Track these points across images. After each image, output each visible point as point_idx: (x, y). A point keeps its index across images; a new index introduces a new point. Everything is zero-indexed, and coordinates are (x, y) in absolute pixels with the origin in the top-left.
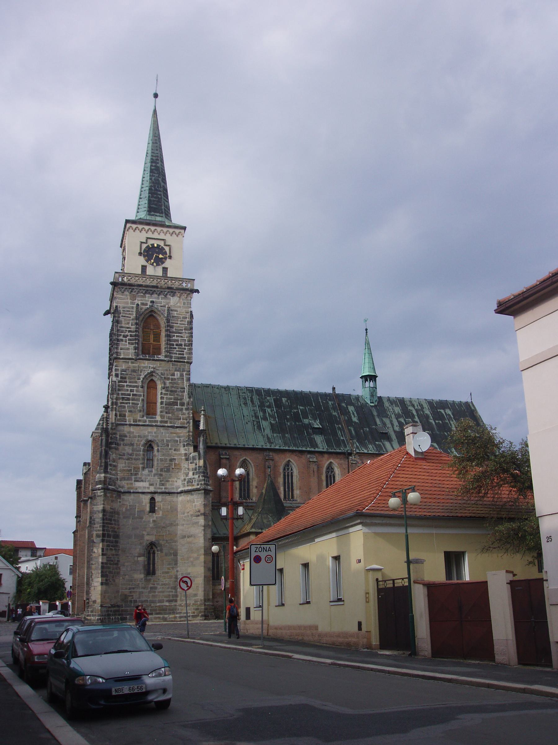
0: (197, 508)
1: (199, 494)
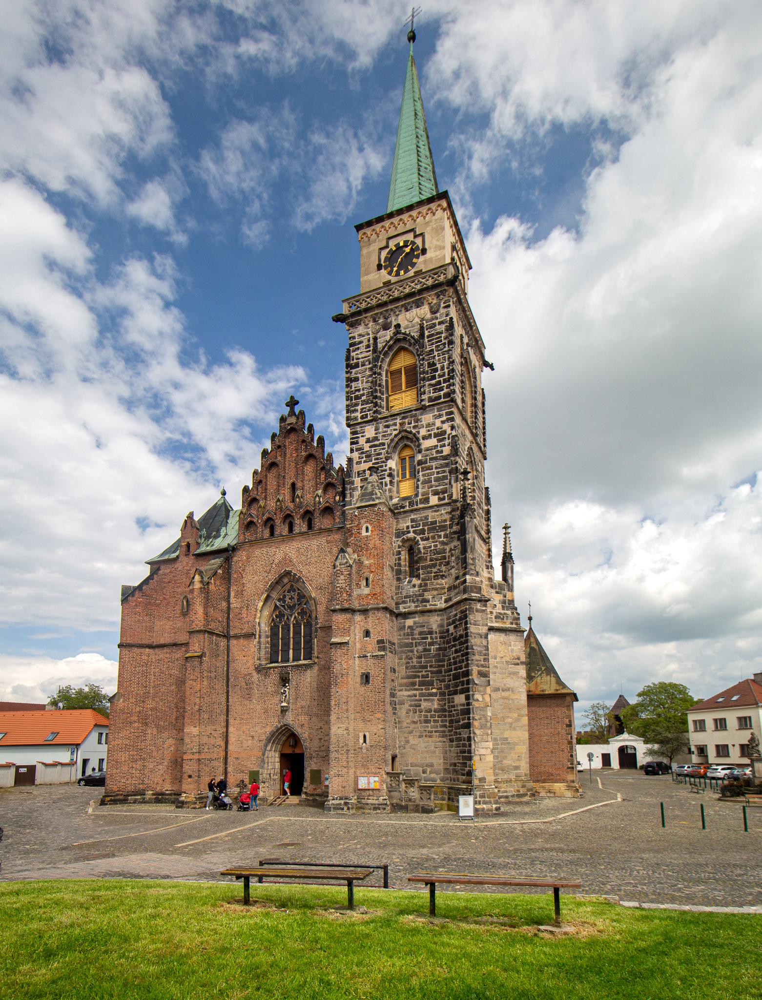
0: (514, 654)
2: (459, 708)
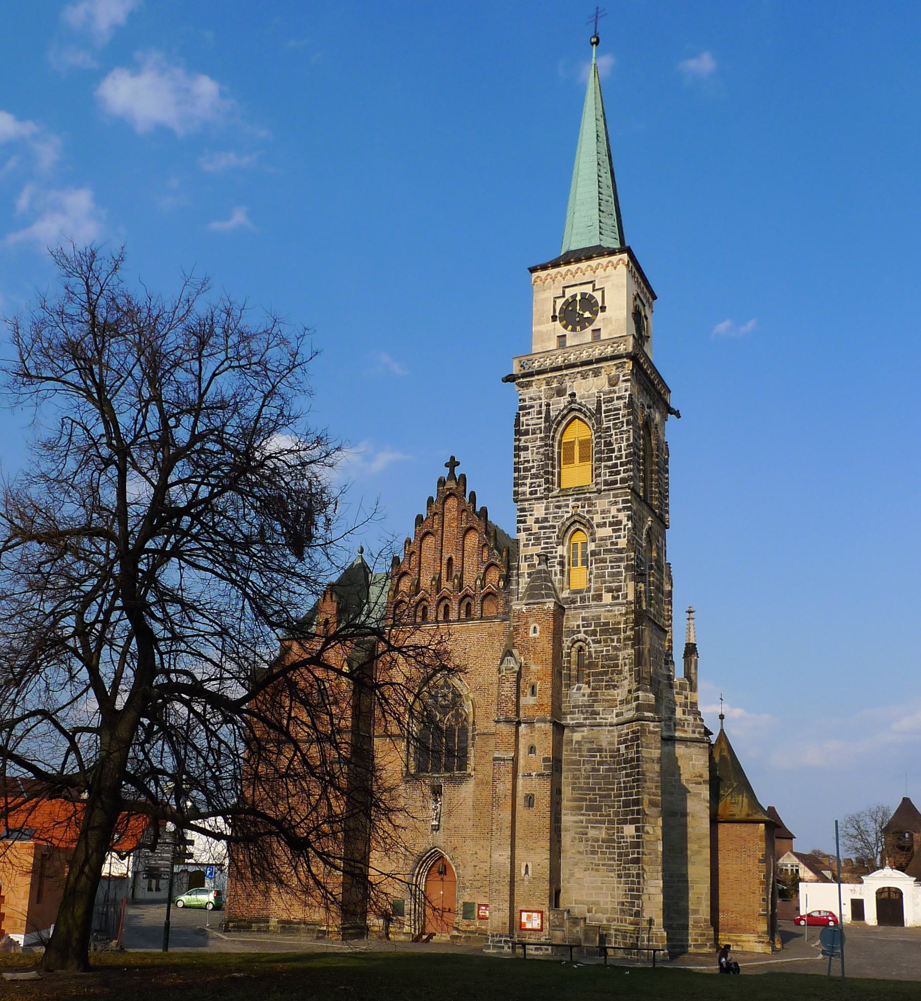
0: (696, 771)
1: (700, 748)
2: (629, 840)
